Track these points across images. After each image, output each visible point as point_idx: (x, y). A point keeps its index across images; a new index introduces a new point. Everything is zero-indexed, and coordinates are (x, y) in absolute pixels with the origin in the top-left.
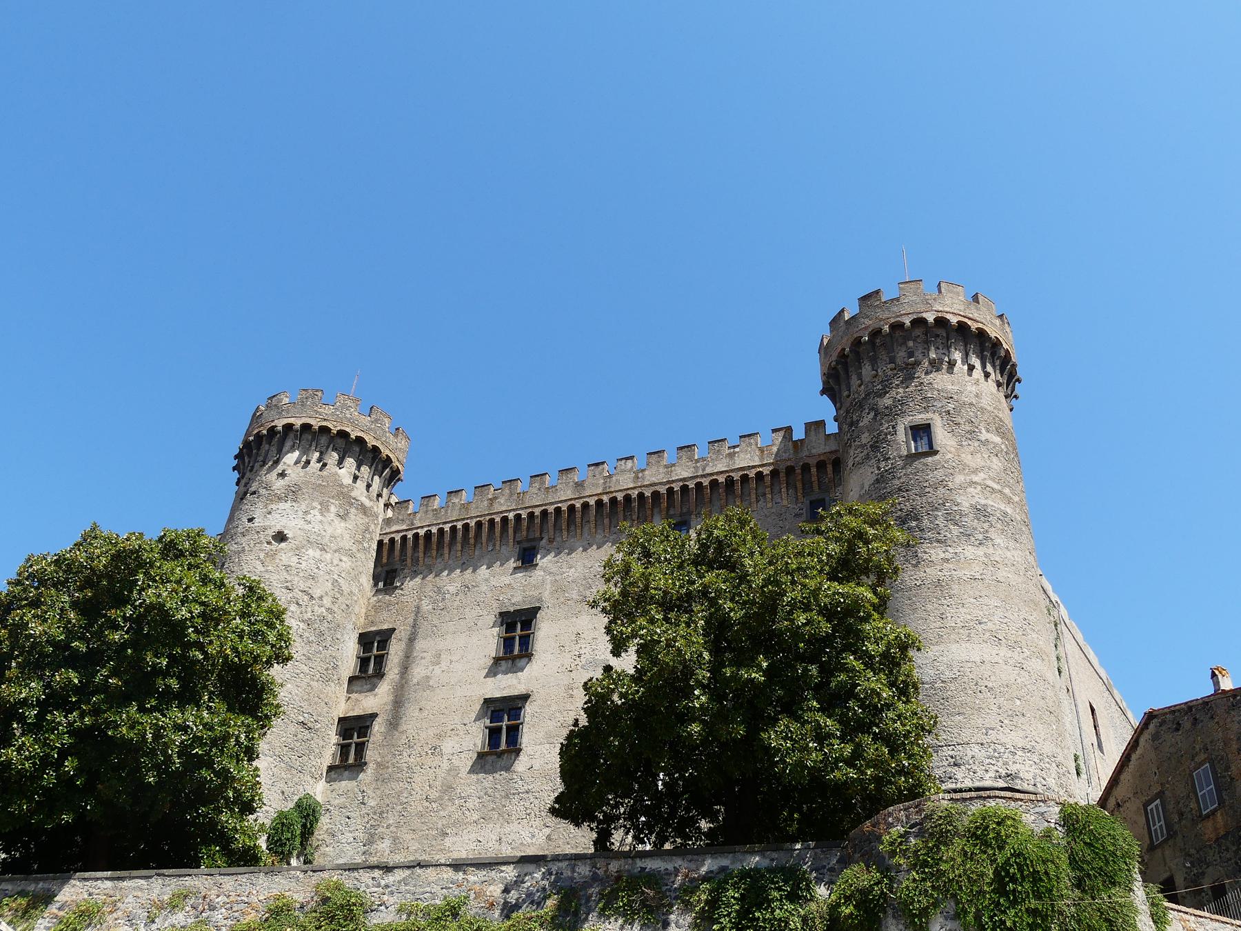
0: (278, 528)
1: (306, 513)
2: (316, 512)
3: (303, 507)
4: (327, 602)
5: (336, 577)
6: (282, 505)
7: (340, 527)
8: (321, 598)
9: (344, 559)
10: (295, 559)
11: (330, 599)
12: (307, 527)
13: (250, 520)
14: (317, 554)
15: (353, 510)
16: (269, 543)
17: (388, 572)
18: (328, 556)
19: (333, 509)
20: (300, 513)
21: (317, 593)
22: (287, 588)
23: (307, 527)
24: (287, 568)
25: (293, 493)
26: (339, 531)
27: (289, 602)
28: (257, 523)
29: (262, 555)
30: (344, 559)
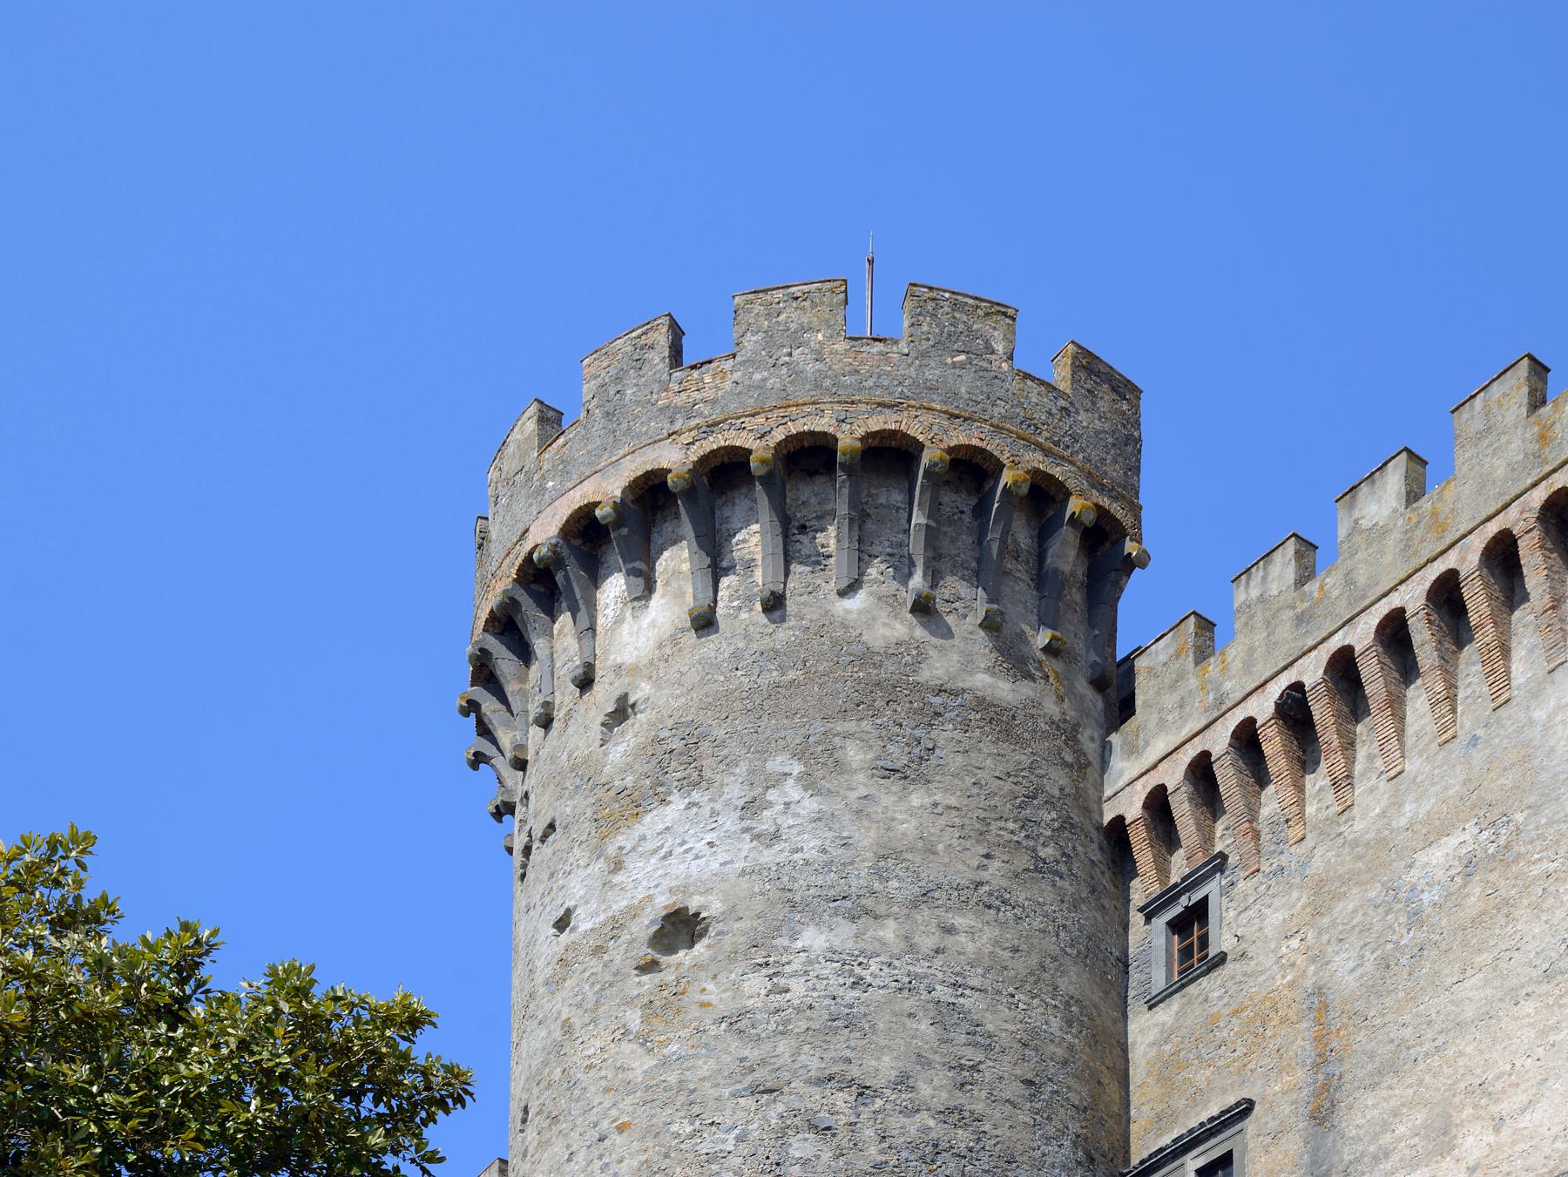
0: (663, 902)
1: (751, 807)
2: (793, 791)
3: (735, 791)
4: (933, 1088)
5: (943, 993)
6: (655, 821)
7: (909, 811)
8: (903, 1082)
9: (958, 921)
10: (756, 984)
11: (943, 1077)
12: (769, 856)
13: (562, 924)
14: (843, 935)
15: (945, 734)
16: (650, 967)
17: (1179, 926)
18: (889, 932)
19: (855, 755)
20: (730, 821)
21: (882, 1067)
22: (757, 1090)
23: (769, 856)
24: (736, 1022)
25: (681, 762)
26: (908, 827)
27: (782, 1133)
28: (584, 922)
29: (634, 1018)
30: (958, 921)
